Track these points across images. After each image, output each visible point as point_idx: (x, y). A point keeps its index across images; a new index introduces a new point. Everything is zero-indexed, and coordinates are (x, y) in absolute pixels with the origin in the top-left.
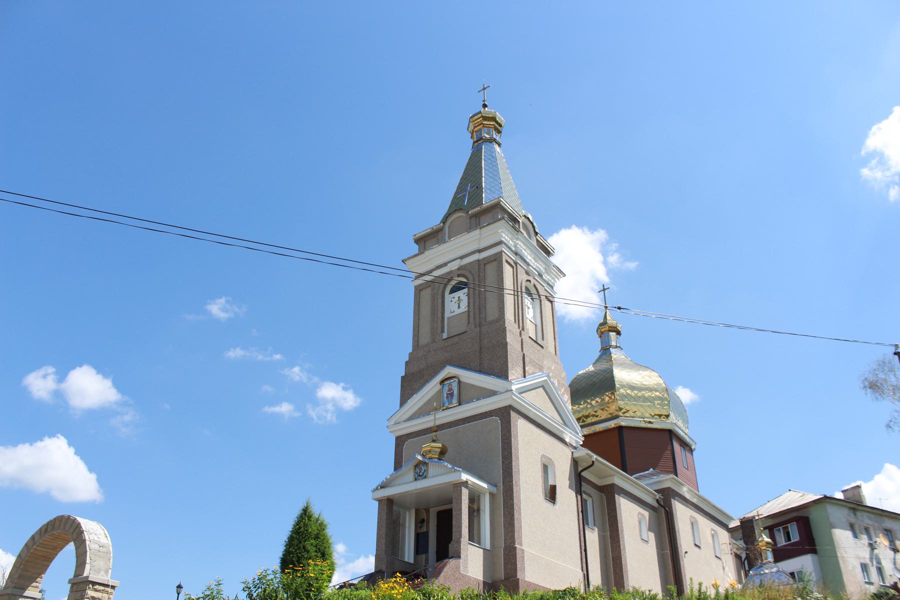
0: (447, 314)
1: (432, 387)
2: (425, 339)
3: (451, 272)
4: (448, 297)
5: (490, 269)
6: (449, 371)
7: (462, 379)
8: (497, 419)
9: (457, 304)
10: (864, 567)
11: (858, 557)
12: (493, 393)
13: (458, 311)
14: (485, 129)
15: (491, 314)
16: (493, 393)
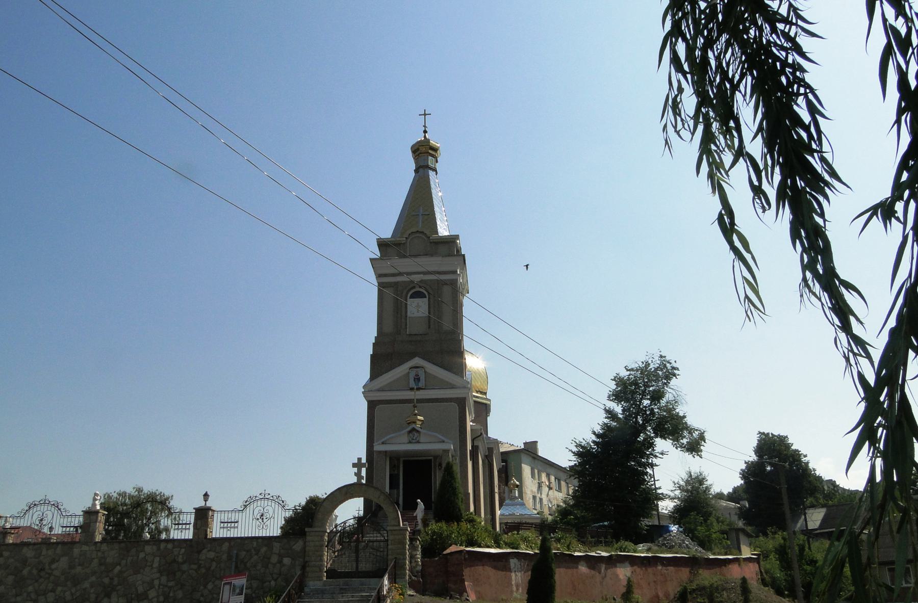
0: (409, 314)
1: (403, 369)
2: (389, 328)
3: (412, 282)
4: (410, 301)
5: (446, 290)
6: (417, 361)
7: (427, 370)
8: (455, 406)
9: (417, 308)
10: (534, 497)
11: (532, 491)
12: (453, 387)
13: (416, 315)
14: (424, 153)
15: (447, 325)
16: (453, 387)
